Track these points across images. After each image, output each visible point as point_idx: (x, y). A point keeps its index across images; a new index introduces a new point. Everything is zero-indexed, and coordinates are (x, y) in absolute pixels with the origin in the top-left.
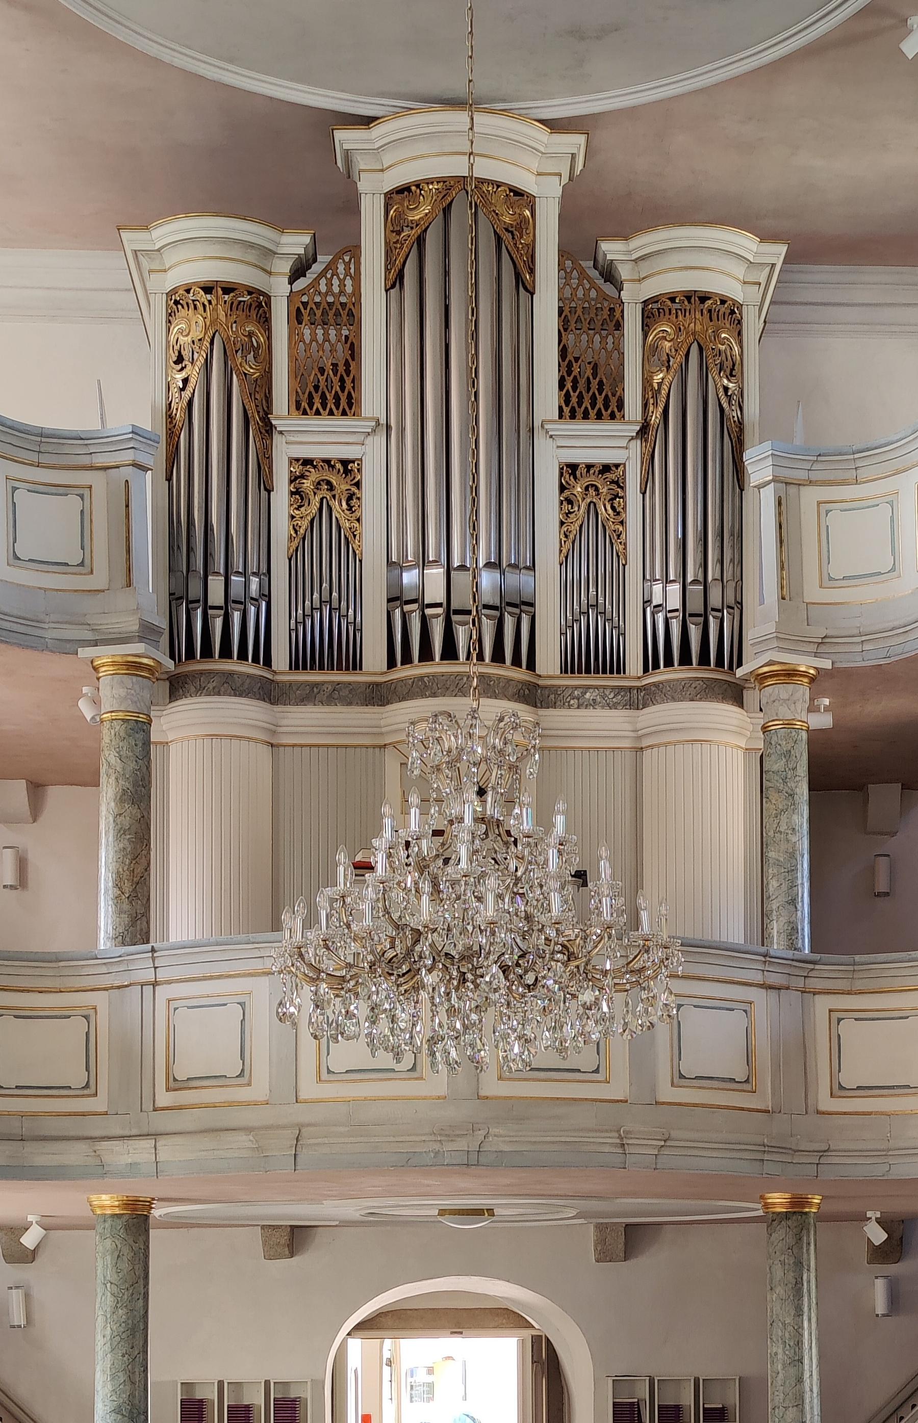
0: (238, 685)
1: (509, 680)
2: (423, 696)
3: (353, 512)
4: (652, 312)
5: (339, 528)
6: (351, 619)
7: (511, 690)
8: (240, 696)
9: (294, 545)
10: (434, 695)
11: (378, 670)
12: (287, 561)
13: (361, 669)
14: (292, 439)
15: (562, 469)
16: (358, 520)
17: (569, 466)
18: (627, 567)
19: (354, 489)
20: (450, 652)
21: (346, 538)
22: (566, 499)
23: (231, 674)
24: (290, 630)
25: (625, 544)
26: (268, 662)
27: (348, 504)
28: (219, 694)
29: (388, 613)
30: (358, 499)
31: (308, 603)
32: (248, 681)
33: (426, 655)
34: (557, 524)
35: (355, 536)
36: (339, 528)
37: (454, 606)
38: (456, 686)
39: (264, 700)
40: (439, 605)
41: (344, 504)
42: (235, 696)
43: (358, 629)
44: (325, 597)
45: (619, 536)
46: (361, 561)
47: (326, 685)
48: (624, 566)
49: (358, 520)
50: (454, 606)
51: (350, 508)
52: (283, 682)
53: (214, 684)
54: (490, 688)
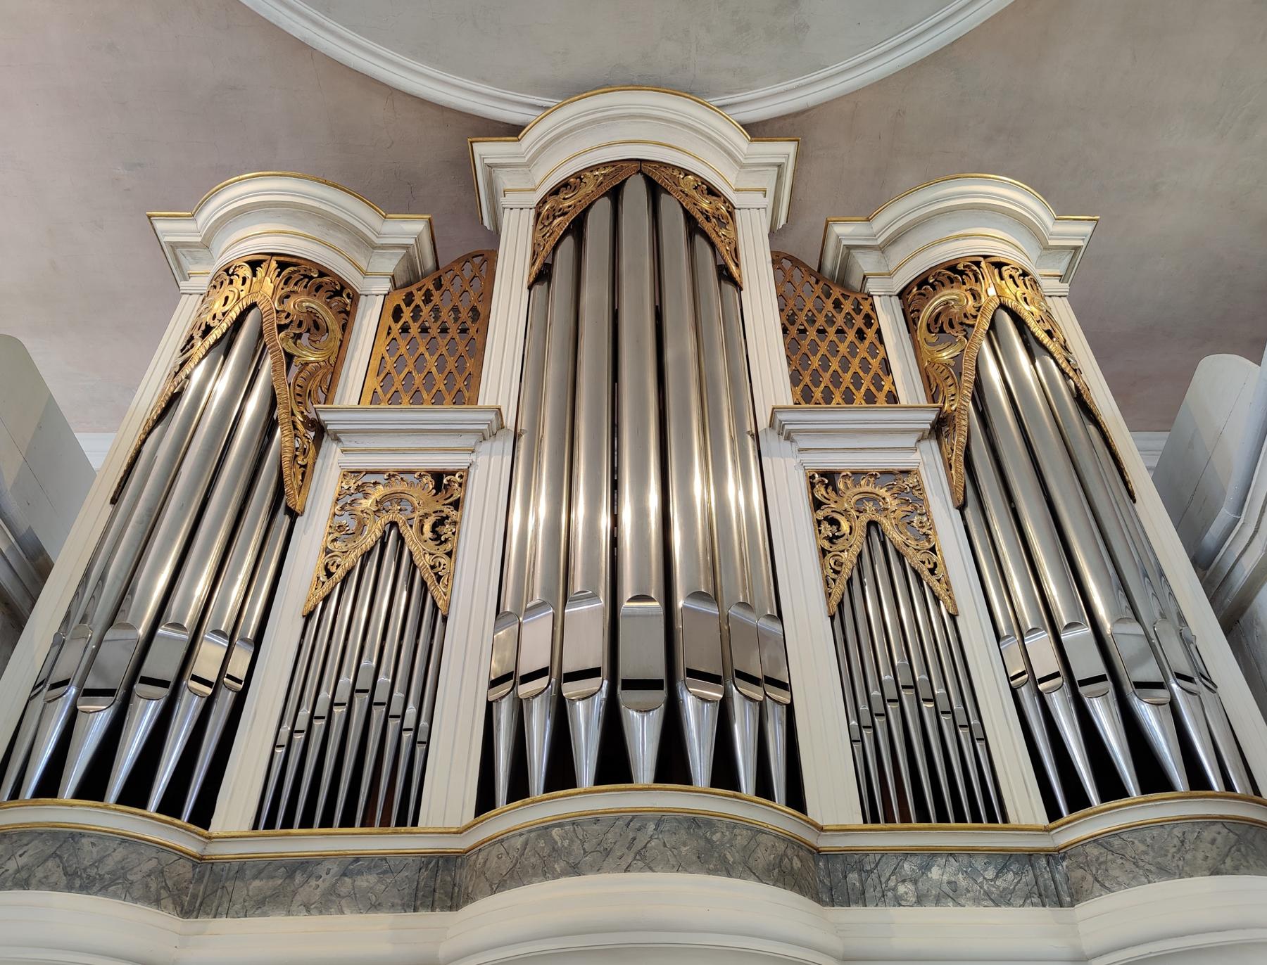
0: (87, 863)
1: (757, 831)
2: (546, 872)
3: (442, 543)
4: (914, 295)
5: (413, 567)
6: (410, 722)
7: (763, 857)
8: (85, 888)
9: (322, 592)
10: (575, 870)
11: (455, 824)
12: (302, 621)
13: (415, 823)
14: (353, 445)
15: (812, 477)
16: (449, 554)
17: (824, 474)
18: (959, 620)
19: (448, 511)
20: (614, 767)
21: (424, 583)
22: (826, 518)
23: (73, 836)
24: (275, 746)
25: (947, 583)
26: (203, 815)
27: (433, 530)
28: (24, 884)
29: (489, 705)
30: (455, 523)
31: (325, 695)
32: (120, 853)
33: (561, 775)
34: (814, 555)
35: (439, 578)
36: (413, 567)
37: (625, 672)
38: (629, 846)
39: (157, 902)
40: (593, 673)
41: (427, 527)
42: (70, 888)
43: (421, 741)
44: (365, 682)
45: (932, 571)
46: (445, 619)
47: (327, 865)
48: (953, 617)
49: (449, 554)
50: (625, 672)
51: (437, 537)
52: (226, 861)
53: (22, 861)
54: (708, 849)
